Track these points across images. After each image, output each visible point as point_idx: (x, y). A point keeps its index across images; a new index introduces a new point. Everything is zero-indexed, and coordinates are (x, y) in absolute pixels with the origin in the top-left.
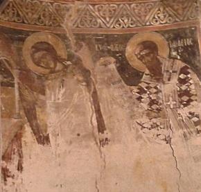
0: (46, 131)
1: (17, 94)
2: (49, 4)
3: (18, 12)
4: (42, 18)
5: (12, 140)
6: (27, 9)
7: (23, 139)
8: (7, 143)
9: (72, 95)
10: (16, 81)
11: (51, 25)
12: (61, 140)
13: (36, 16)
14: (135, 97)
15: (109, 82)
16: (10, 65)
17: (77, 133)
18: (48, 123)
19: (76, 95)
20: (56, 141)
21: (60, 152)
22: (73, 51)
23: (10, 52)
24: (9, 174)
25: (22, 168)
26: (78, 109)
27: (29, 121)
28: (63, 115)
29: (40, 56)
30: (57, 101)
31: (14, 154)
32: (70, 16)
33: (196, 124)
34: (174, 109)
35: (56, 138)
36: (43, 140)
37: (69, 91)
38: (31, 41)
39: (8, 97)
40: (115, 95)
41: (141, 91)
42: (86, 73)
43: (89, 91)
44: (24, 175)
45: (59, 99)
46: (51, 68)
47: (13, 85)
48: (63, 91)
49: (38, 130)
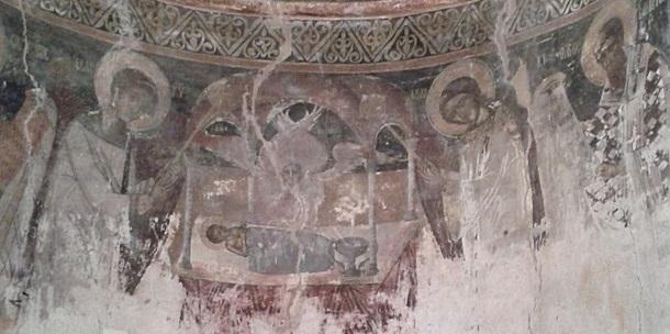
0: (457, 234)
1: (411, 177)
2: (473, 6)
3: (418, 40)
4: (460, 35)
5: (400, 258)
6: (434, 29)
7: (418, 253)
8: (389, 263)
9: (499, 161)
10: (411, 155)
11: (473, 45)
12: (479, 247)
13: (449, 37)
14: (588, 141)
15: (554, 123)
16: (400, 132)
17: (504, 229)
18: (462, 221)
19: (505, 160)
20: (472, 249)
21: (477, 268)
22: (505, 81)
23: (403, 111)
24: (392, 314)
25: (414, 302)
26: (508, 187)
27: (430, 222)
28: (485, 202)
29: (456, 103)
30: (478, 178)
31: (402, 278)
32: (504, 16)
33: (664, 174)
34: (636, 153)
35: (472, 243)
36: (451, 249)
37: (495, 155)
38: (440, 83)
39: (394, 186)
40: (561, 144)
41: (598, 127)
42: (521, 113)
43: (525, 145)
44: (419, 313)
45: (480, 173)
46: (471, 122)
47: (404, 166)
48: (486, 157)
49: (444, 233)
